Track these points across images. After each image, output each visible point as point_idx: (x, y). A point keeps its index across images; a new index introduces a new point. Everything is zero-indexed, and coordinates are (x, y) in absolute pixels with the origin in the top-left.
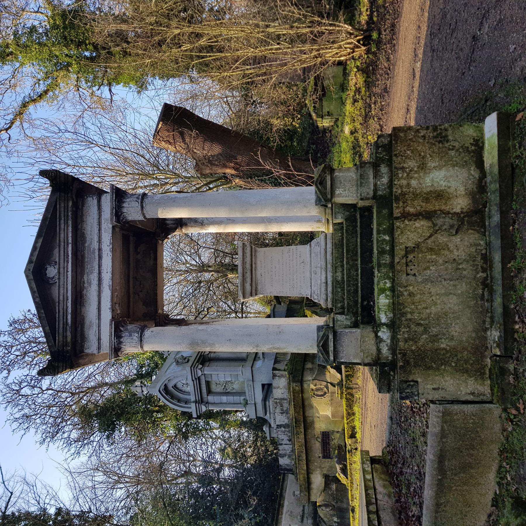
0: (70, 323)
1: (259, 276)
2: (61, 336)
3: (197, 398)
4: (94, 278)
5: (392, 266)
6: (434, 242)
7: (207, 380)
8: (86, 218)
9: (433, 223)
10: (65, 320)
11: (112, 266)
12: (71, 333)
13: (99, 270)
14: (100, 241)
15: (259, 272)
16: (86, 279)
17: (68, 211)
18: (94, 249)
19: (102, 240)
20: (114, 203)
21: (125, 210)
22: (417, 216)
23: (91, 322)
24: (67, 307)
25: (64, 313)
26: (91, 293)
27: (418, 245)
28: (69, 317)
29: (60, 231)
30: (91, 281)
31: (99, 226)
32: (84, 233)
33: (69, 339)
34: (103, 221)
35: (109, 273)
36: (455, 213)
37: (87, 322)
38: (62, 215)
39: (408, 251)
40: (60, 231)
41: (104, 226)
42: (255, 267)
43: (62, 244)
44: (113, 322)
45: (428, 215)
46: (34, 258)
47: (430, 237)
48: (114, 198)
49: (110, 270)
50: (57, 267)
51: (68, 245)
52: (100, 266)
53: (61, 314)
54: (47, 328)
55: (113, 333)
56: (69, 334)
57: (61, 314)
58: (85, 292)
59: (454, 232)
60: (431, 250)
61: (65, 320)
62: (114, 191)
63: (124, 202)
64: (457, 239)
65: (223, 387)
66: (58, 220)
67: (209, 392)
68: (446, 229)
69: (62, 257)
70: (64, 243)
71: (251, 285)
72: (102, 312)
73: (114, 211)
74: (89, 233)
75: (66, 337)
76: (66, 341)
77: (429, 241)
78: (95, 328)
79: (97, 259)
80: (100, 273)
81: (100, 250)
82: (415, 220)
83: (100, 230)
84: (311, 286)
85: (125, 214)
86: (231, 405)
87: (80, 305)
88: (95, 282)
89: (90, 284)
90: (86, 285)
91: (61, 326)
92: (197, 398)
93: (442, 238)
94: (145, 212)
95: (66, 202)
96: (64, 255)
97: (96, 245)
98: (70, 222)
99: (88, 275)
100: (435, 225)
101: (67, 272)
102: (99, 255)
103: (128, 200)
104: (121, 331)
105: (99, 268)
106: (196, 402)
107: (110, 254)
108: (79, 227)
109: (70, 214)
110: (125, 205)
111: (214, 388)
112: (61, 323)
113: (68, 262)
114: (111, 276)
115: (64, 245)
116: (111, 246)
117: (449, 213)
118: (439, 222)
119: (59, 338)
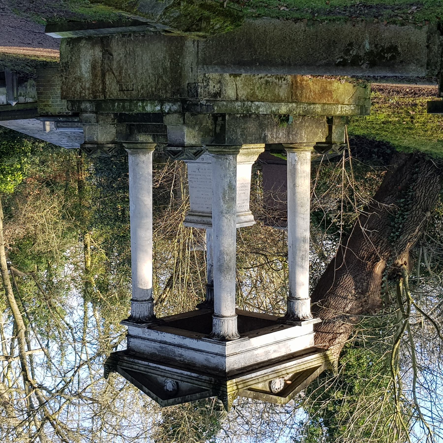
5: (131, 101)
6: (116, 71)
9: (107, 72)
11: (171, 334)
20: (130, 323)
22: (104, 83)
24: (187, 375)
25: (189, 378)
26: (188, 355)
27: (118, 82)
30: (180, 354)
35: (175, 337)
36: (102, 56)
39: (121, 90)
45: (104, 75)
47: (114, 74)
51: (149, 366)
59: (111, 57)
60: (120, 73)
64: (115, 54)
68: (110, 63)
69: (155, 372)
70: (147, 368)
72: (200, 349)
73: (135, 324)
77: (116, 74)
81: (161, 342)
82: (106, 84)
85: (141, 316)
87: (194, 367)
90: (182, 359)
93: (115, 66)
94: (141, 299)
96: (154, 370)
99: (175, 356)
100: (108, 70)
101: (165, 370)
102: (163, 343)
105: (171, 345)
107: (164, 334)
113: (159, 368)
114: (177, 336)
115: (149, 368)
116: (159, 332)
117: (102, 61)
118: (106, 67)
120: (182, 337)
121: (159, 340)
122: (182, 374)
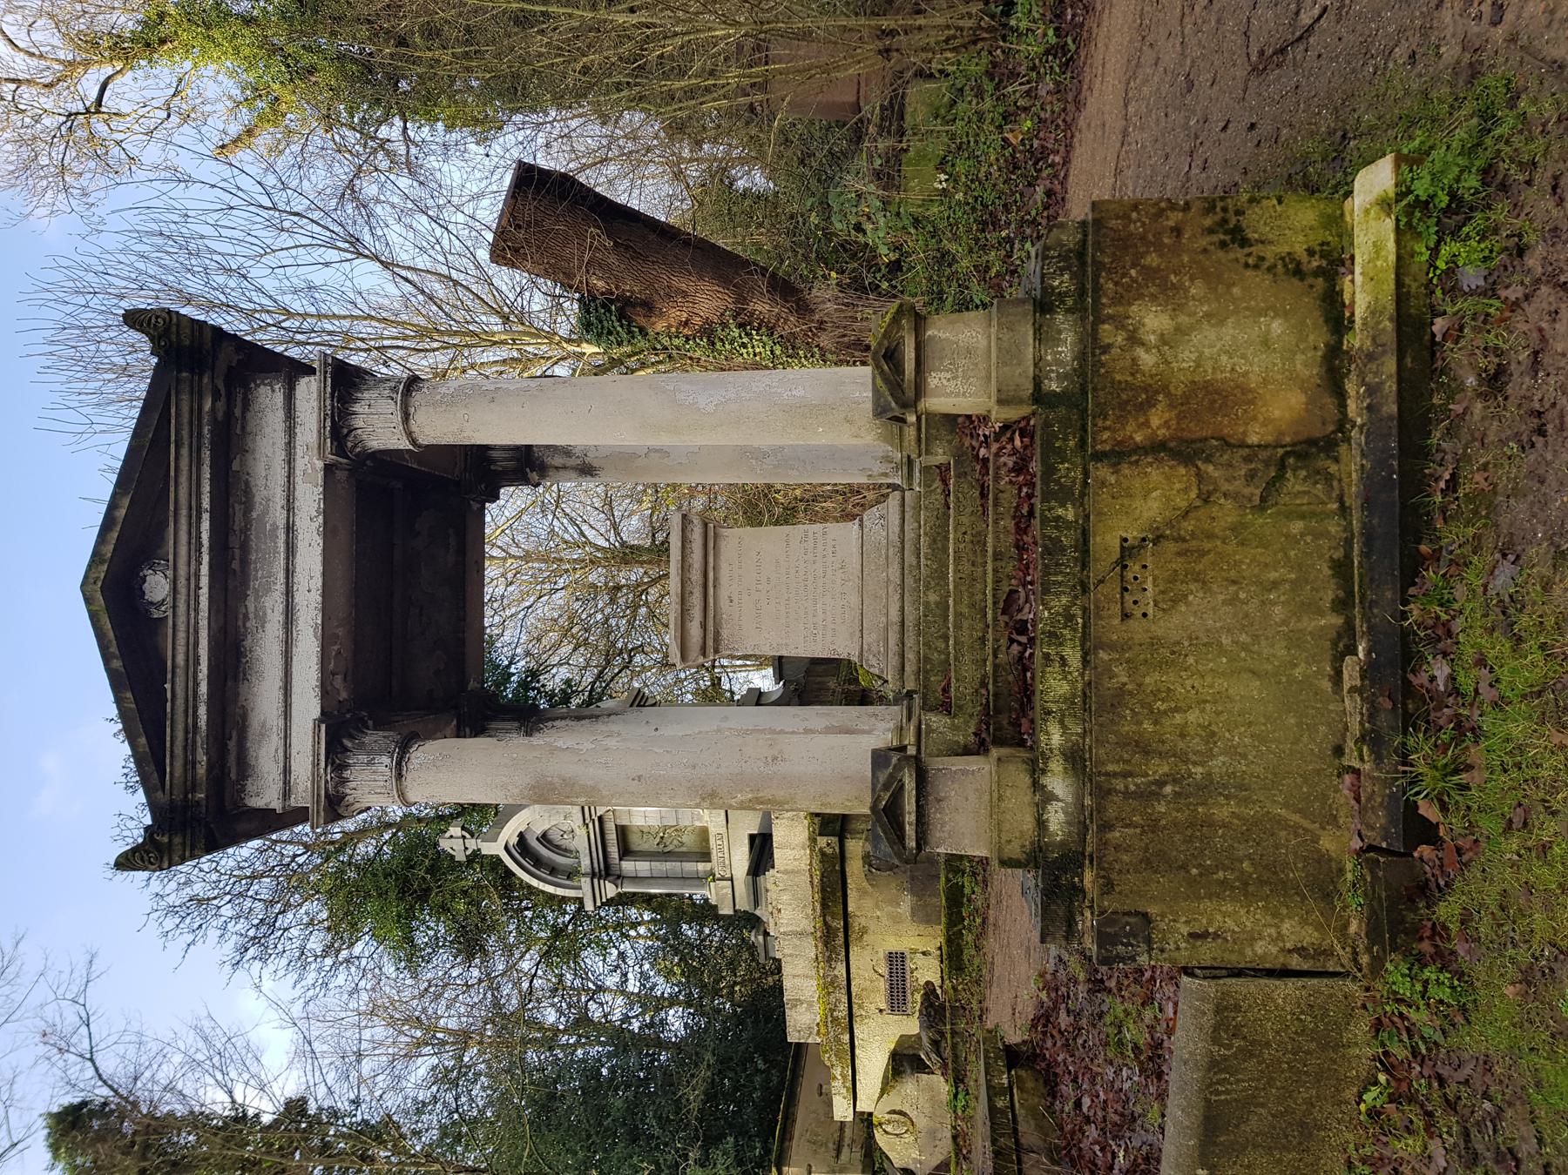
0: (204, 728)
1: (724, 603)
2: (179, 764)
3: (596, 865)
4: (273, 604)
7: (619, 822)
8: (254, 441)
10: (190, 721)
11: (324, 574)
12: (207, 754)
13: (287, 584)
14: (290, 507)
15: (724, 593)
16: (251, 609)
17: (200, 419)
18: (275, 528)
19: (297, 504)
20: (328, 402)
21: (358, 422)
23: (263, 725)
28: (202, 711)
29: (176, 476)
31: (289, 463)
32: (247, 483)
33: (201, 771)
34: (299, 451)
37: (255, 722)
38: (185, 433)
40: (176, 476)
41: (300, 464)
42: (716, 579)
43: (184, 512)
44: (323, 727)
46: (108, 550)
48: (329, 389)
49: (317, 582)
50: (170, 573)
51: (199, 518)
52: (289, 573)
53: (180, 701)
54: (143, 740)
55: (323, 758)
56: (202, 758)
57: (180, 701)
58: (248, 643)
61: (190, 721)
62: (329, 369)
63: (356, 400)
65: (658, 840)
66: (173, 446)
67: (626, 852)
71: (704, 626)
73: (328, 423)
74: (261, 482)
75: (194, 763)
76: (194, 777)
78: (274, 742)
79: (282, 556)
80: (289, 592)
81: (290, 528)
83: (290, 476)
84: (862, 631)
85: (359, 431)
86: (677, 882)
87: (236, 679)
88: (275, 618)
89: (262, 621)
90: (251, 624)
91: (180, 735)
92: (596, 865)
94: (414, 428)
95: (196, 396)
97: (279, 516)
98: (206, 455)
99: (257, 598)
101: (198, 588)
102: (287, 543)
103: (366, 395)
104: (346, 750)
105: (287, 578)
106: (593, 875)
108: (235, 466)
109: (206, 430)
110: (357, 408)
111: (636, 842)
112: (180, 727)
114: (319, 599)
115: (190, 517)
119: (175, 768)
120: (319, 622)
121: (298, 522)
122: (197, 662)
